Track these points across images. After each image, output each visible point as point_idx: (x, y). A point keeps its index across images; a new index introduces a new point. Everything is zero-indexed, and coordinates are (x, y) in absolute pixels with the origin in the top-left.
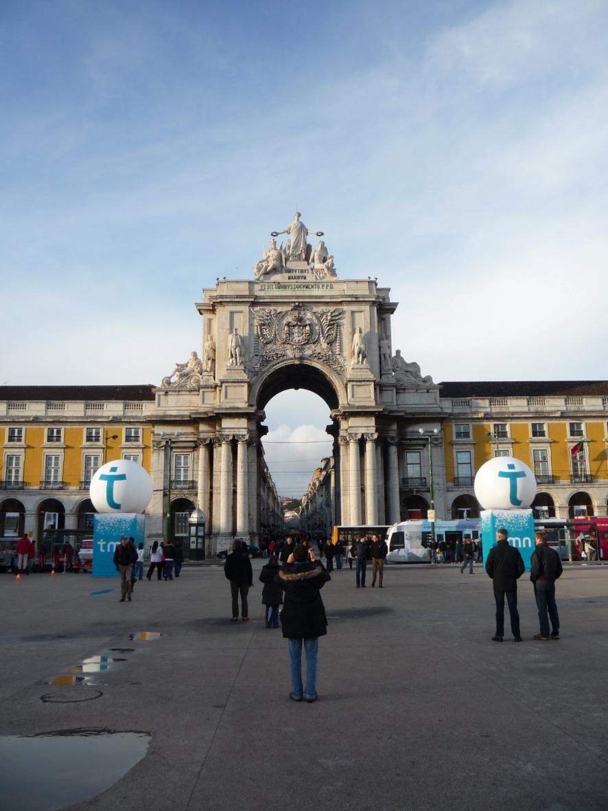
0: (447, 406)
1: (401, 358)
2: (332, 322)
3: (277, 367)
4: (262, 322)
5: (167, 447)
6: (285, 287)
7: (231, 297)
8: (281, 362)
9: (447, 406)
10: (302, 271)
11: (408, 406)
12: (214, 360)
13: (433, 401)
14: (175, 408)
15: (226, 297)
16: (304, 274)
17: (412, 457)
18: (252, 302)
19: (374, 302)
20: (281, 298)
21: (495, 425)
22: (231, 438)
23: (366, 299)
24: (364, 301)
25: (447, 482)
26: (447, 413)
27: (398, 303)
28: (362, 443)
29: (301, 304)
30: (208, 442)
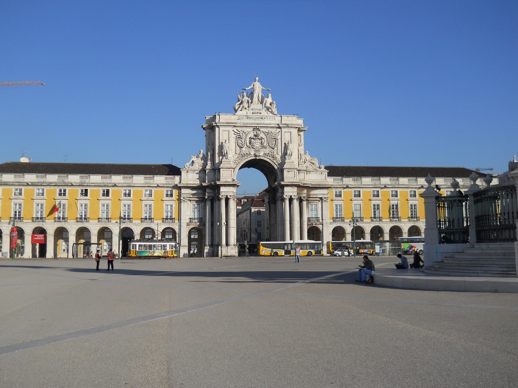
4: (240, 137)
8: (249, 157)
9: (331, 181)
10: (259, 110)
11: (312, 181)
14: (192, 180)
19: (296, 127)
28: (291, 200)
30: (211, 198)
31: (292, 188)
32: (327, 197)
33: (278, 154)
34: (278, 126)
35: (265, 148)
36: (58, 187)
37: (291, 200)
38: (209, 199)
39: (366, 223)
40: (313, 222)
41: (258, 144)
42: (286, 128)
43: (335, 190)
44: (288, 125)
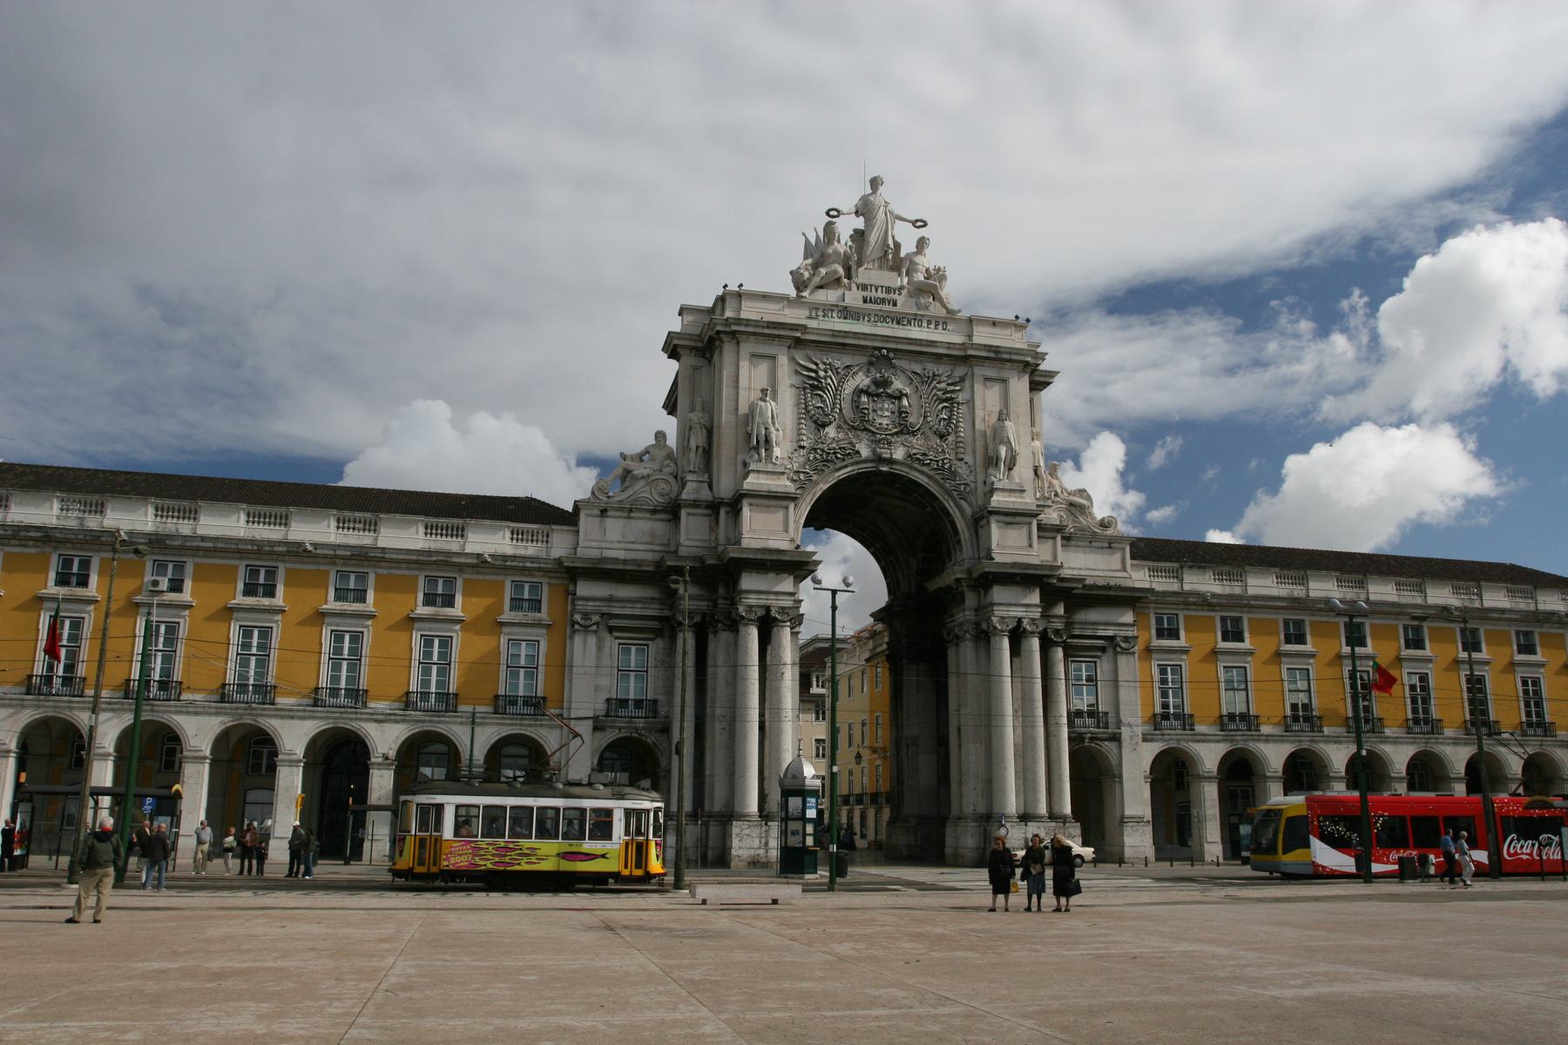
0: (1139, 577)
5: (601, 626)
7: (756, 323)
10: (888, 290)
12: (707, 453)
14: (622, 545)
15: (748, 322)
16: (891, 296)
19: (1027, 364)
20: (854, 338)
22: (761, 613)
28: (1017, 636)
29: (891, 355)
30: (697, 619)
31: (1020, 589)
32: (1130, 634)
33: (961, 460)
35: (913, 432)
36: (56, 548)
37: (1017, 636)
39: (1268, 739)
40: (1084, 730)
41: (886, 414)
43: (1158, 611)
44: (996, 350)
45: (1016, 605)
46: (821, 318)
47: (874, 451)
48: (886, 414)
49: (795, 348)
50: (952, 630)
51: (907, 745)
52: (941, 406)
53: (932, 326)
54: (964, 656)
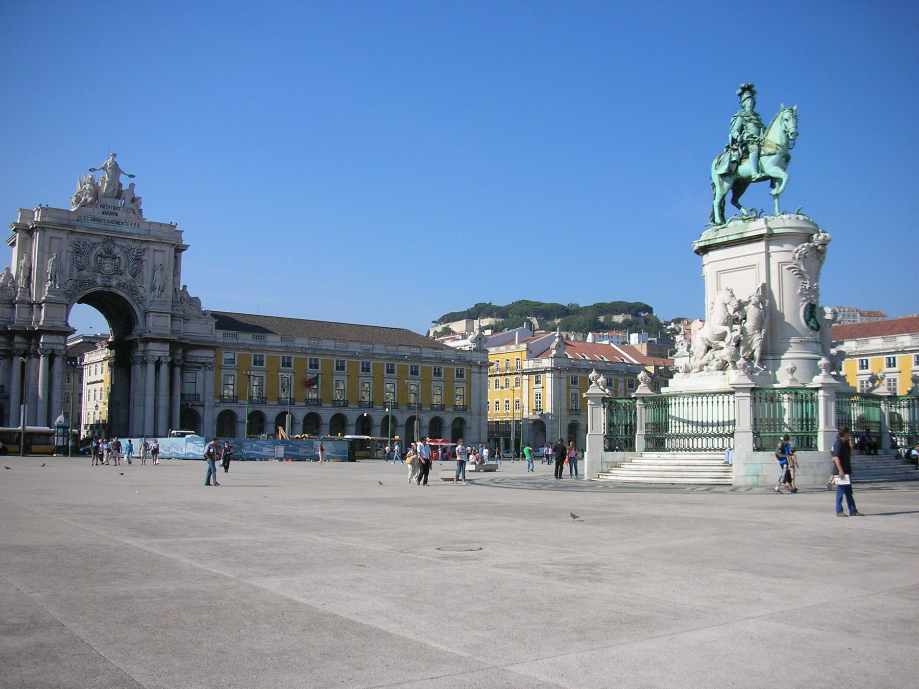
1: (187, 292)
2: (137, 258)
3: (88, 291)
6: (99, 220)
8: (93, 287)
10: (114, 208)
11: (190, 334)
12: (29, 279)
13: (210, 332)
17: (189, 376)
18: (72, 232)
19: (174, 244)
21: (255, 355)
22: (50, 352)
23: (167, 242)
24: (166, 243)
25: (215, 399)
26: (220, 343)
27: (189, 246)
28: (158, 364)
33: (141, 286)
34: (145, 240)
37: (158, 364)
38: (18, 353)
40: (189, 402)
41: (110, 265)
42: (156, 244)
45: (159, 351)
46: (83, 220)
47: (102, 281)
48: (110, 265)
49: (70, 234)
50: (133, 359)
51: (115, 405)
52: (133, 262)
53: (133, 225)
54: (137, 369)
